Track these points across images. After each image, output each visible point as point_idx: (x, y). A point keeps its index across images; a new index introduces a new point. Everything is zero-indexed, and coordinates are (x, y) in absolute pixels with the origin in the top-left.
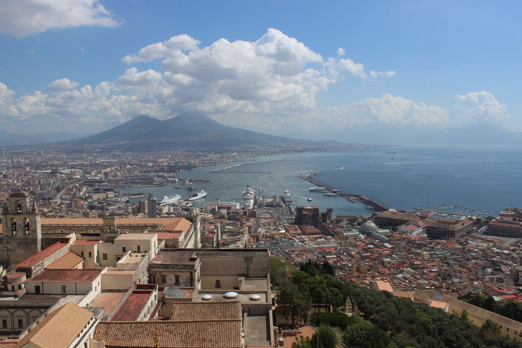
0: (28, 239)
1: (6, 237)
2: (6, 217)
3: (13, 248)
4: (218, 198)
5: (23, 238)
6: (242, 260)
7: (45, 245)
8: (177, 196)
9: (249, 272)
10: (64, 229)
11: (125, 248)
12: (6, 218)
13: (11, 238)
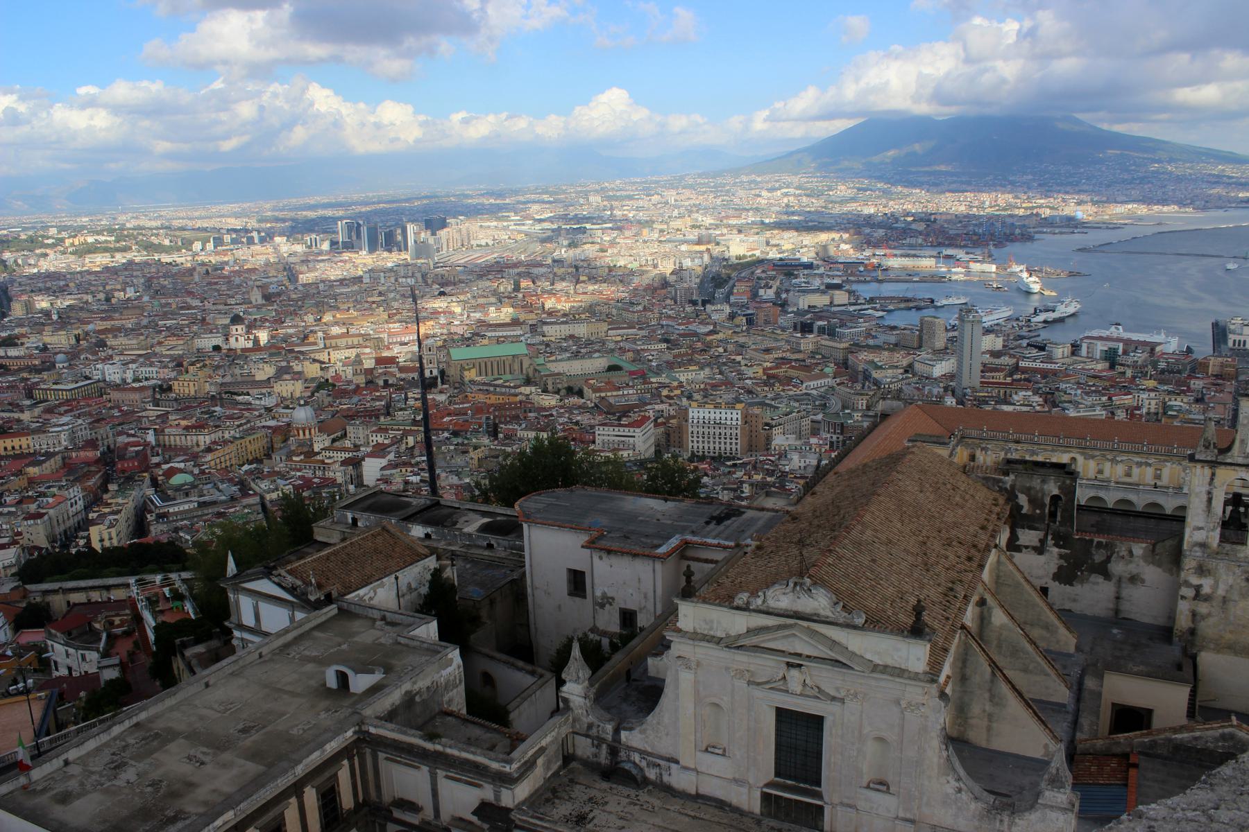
1: (1197, 549)
2: (1213, 474)
4: (1119, 322)
8: (1005, 309)
10: (1082, 454)
12: (1212, 479)
13: (1217, 553)
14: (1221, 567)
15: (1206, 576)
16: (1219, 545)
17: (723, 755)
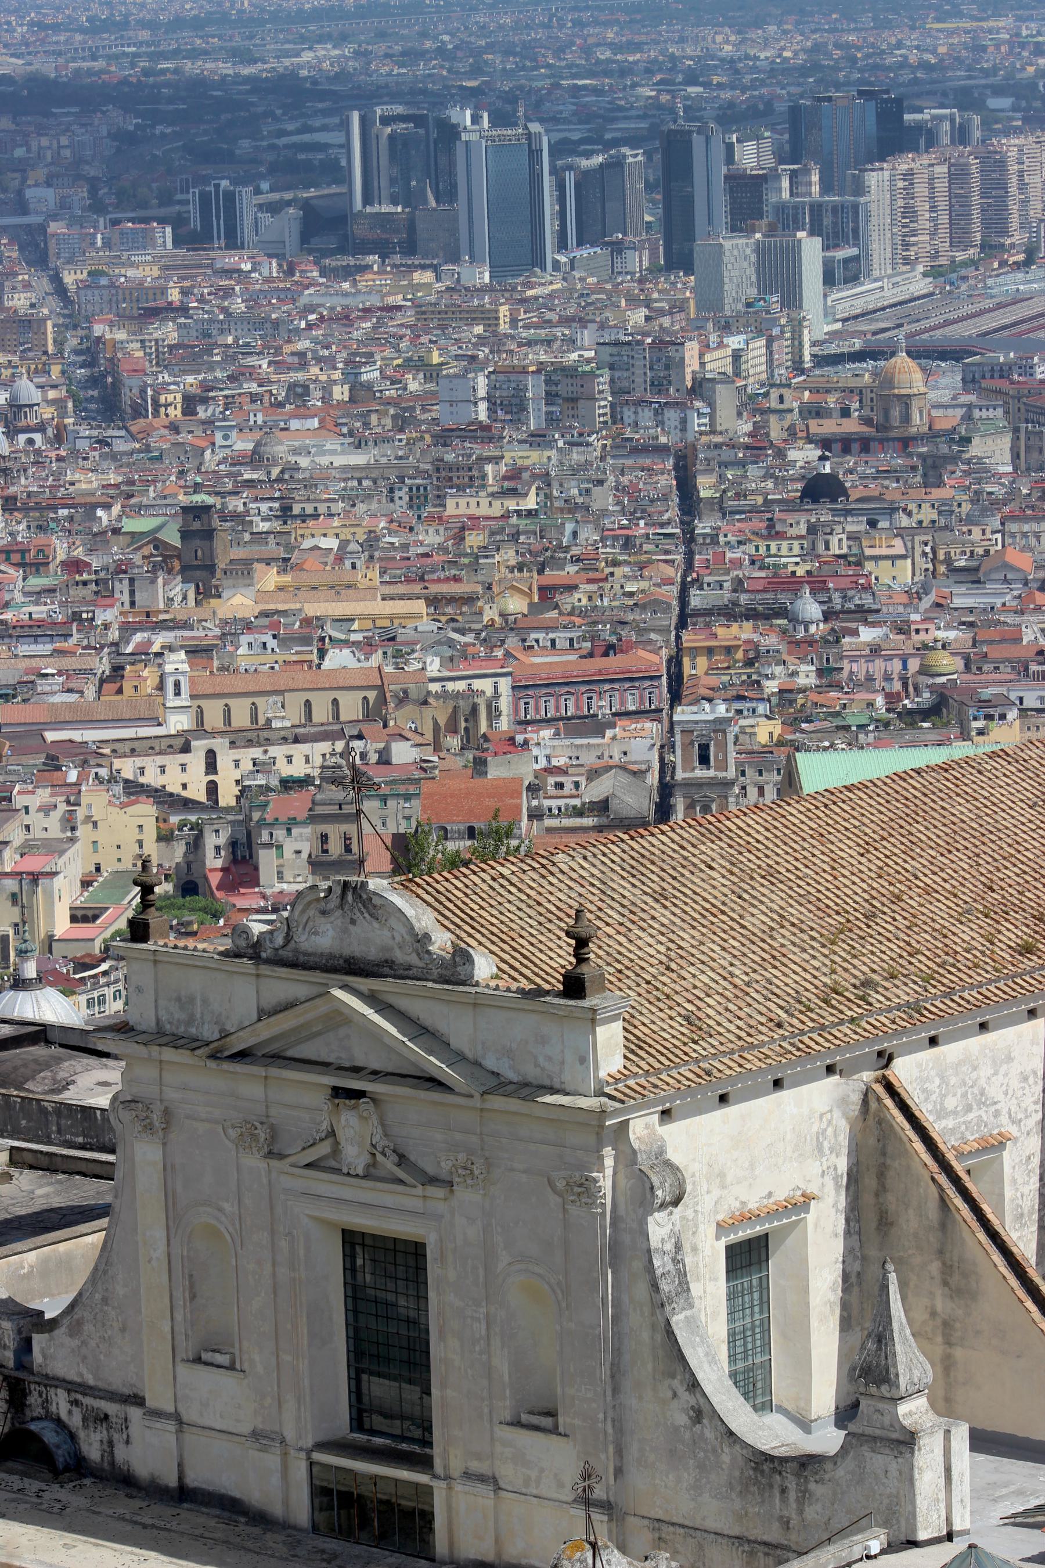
17: (231, 1367)
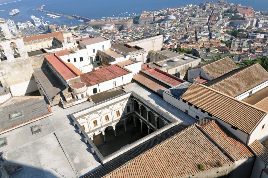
0: (21, 61)
3: (7, 72)
5: (15, 61)
6: (151, 41)
7: (34, 62)
9: (154, 49)
11: (94, 49)
13: (2, 64)
14: (4, 66)
15: (2, 70)
16: (1, 62)
